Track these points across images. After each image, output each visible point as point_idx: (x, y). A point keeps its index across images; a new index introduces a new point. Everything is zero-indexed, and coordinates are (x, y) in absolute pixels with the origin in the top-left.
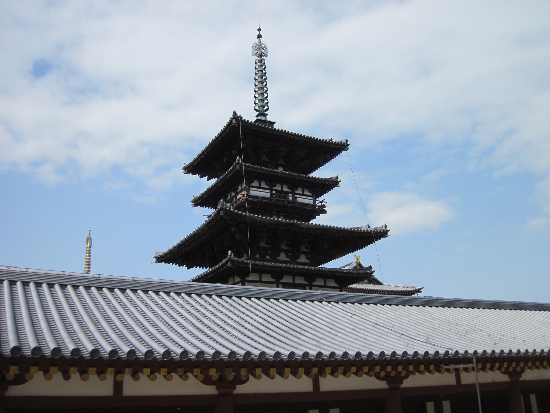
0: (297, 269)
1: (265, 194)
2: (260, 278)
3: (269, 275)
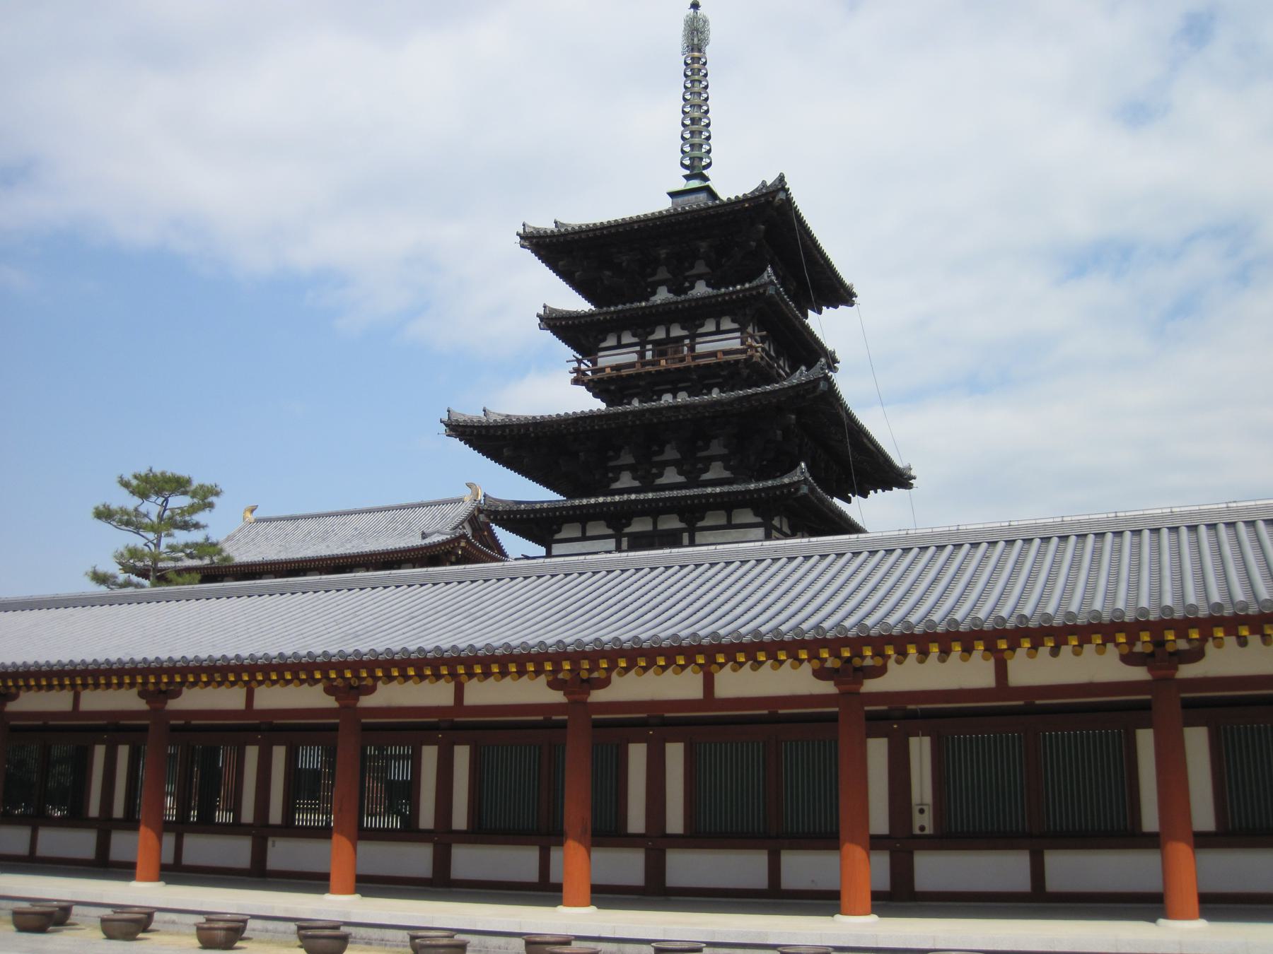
1: (629, 357)
2: (584, 531)
3: (603, 522)
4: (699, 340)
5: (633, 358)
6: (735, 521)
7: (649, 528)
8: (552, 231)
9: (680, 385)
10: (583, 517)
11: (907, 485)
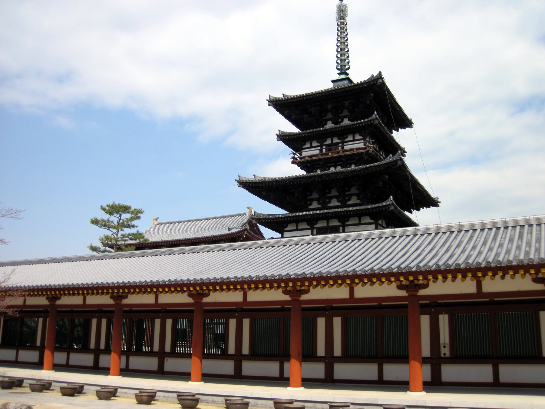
0: (302, 215)
1: (316, 152)
4: (345, 144)
5: (317, 152)
6: (362, 222)
7: (325, 225)
8: (282, 98)
9: (338, 163)
10: (297, 221)
11: (437, 205)
